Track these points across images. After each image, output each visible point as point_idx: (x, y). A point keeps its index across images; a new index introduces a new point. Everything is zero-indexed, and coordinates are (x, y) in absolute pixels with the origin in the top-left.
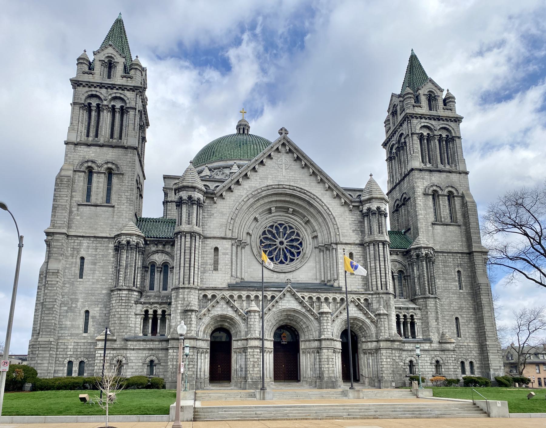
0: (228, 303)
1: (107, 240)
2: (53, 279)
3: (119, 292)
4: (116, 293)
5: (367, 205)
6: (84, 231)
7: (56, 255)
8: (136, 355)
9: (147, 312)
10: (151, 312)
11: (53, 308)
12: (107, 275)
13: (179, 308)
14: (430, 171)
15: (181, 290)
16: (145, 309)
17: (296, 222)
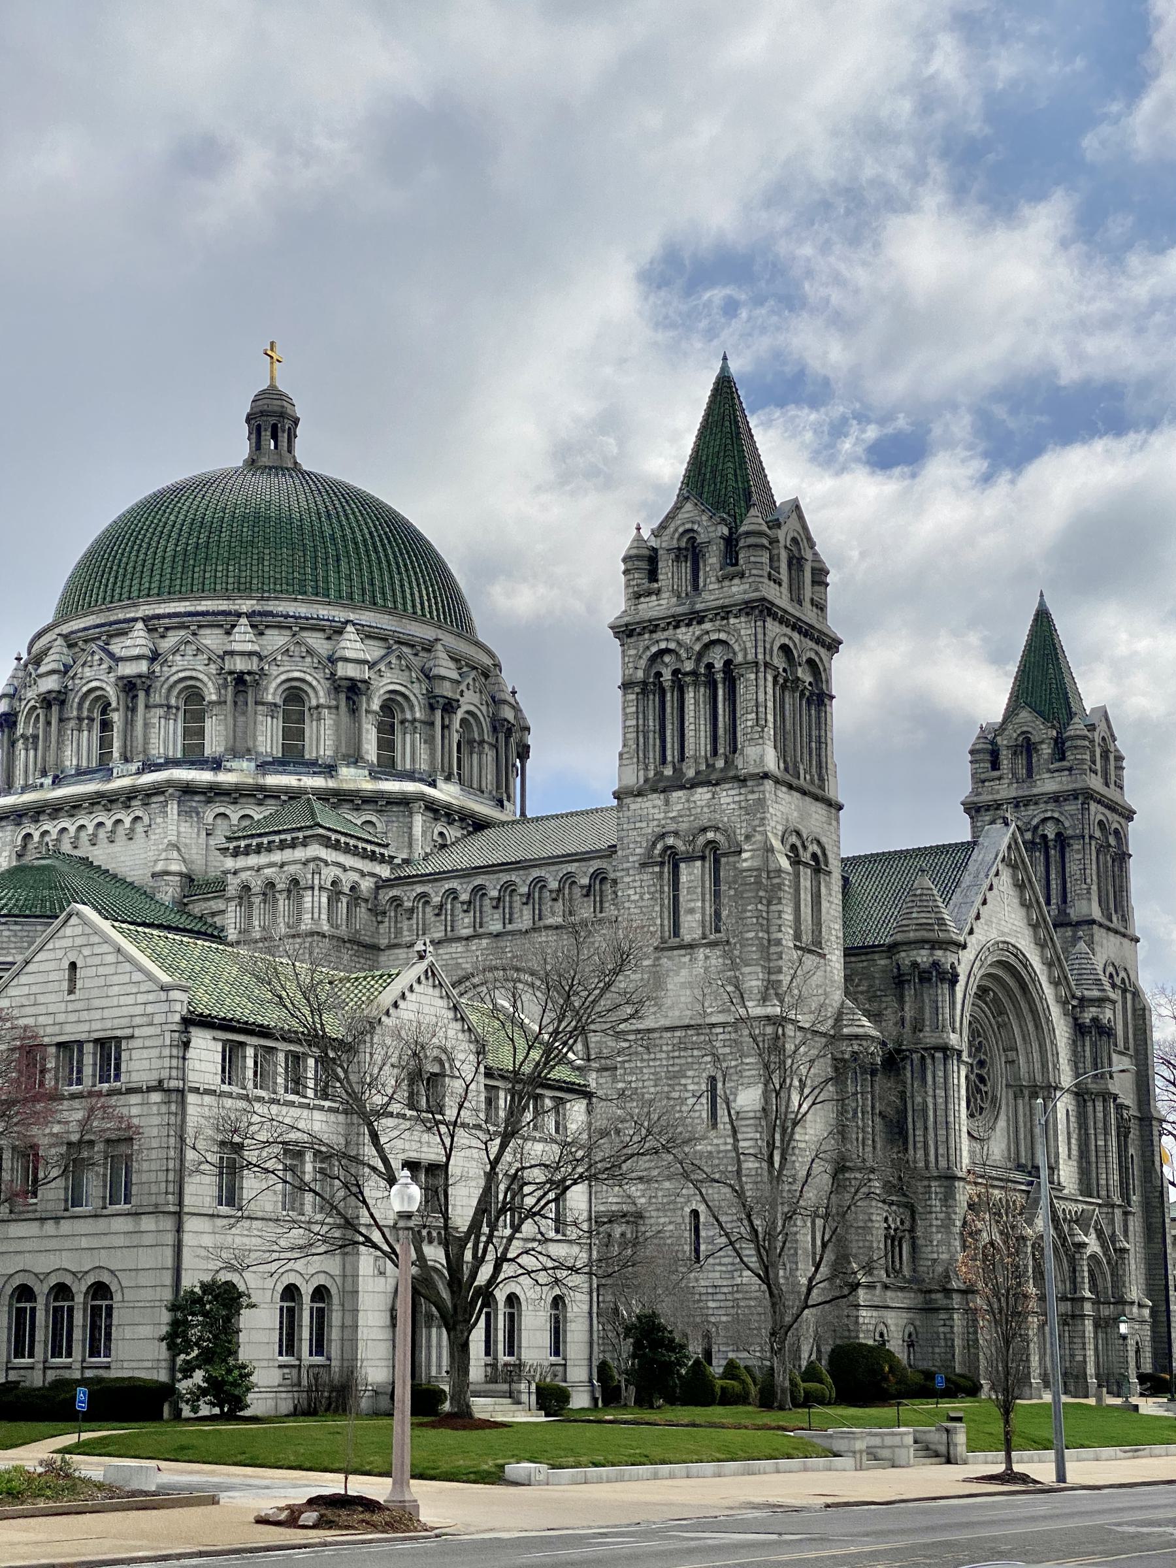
5: (1092, 1009)
14: (1109, 929)
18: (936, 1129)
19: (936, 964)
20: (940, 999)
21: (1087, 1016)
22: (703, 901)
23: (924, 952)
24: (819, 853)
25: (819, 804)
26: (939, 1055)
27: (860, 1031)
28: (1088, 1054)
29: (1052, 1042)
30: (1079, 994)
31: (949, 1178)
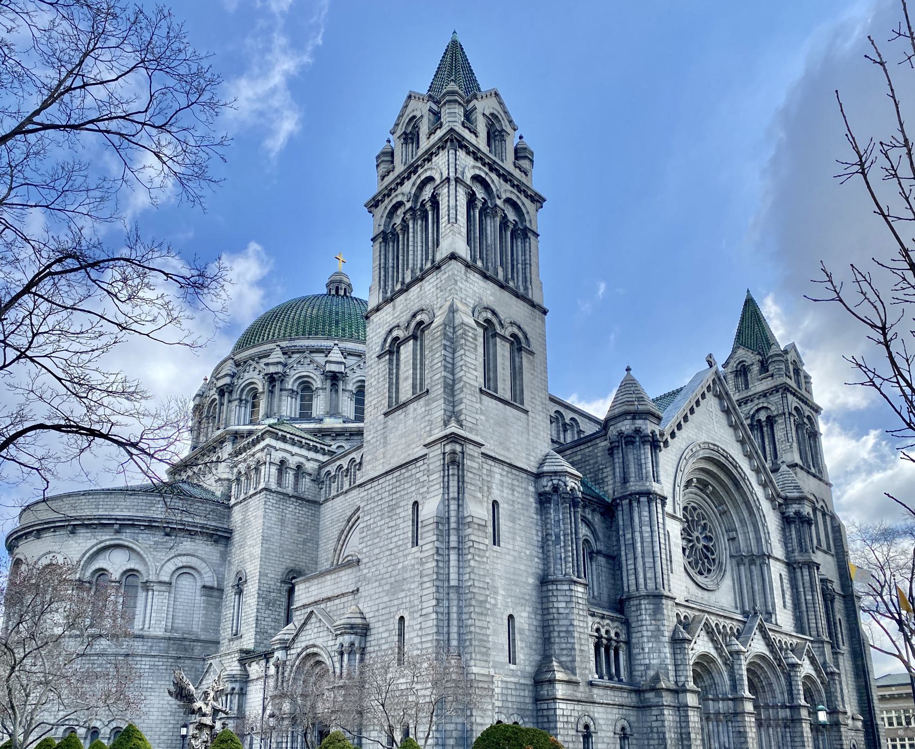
0: (710, 633)
1: (524, 475)
2: (480, 540)
3: (573, 587)
4: (566, 587)
6: (492, 447)
7: (473, 488)
8: (604, 716)
9: (598, 630)
10: (603, 631)
11: (486, 601)
12: (532, 547)
13: (666, 634)
15: (664, 601)
16: (595, 626)
17: (710, 509)
18: (643, 557)
19: (638, 431)
20: (643, 457)
21: (792, 510)
22: (414, 368)
23: (626, 422)
24: (516, 331)
25: (520, 303)
26: (644, 499)
27: (559, 469)
28: (794, 536)
29: (763, 525)
30: (782, 494)
31: (657, 597)
